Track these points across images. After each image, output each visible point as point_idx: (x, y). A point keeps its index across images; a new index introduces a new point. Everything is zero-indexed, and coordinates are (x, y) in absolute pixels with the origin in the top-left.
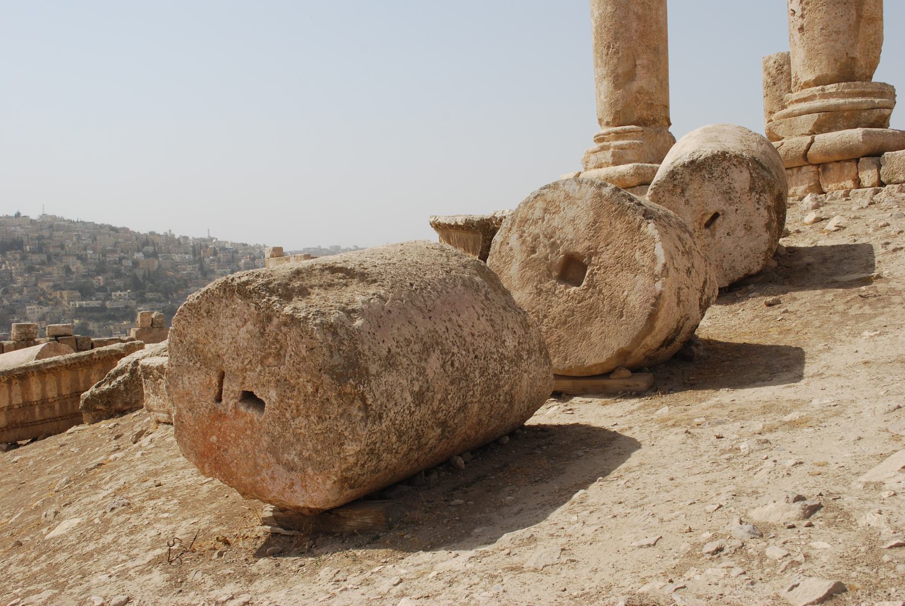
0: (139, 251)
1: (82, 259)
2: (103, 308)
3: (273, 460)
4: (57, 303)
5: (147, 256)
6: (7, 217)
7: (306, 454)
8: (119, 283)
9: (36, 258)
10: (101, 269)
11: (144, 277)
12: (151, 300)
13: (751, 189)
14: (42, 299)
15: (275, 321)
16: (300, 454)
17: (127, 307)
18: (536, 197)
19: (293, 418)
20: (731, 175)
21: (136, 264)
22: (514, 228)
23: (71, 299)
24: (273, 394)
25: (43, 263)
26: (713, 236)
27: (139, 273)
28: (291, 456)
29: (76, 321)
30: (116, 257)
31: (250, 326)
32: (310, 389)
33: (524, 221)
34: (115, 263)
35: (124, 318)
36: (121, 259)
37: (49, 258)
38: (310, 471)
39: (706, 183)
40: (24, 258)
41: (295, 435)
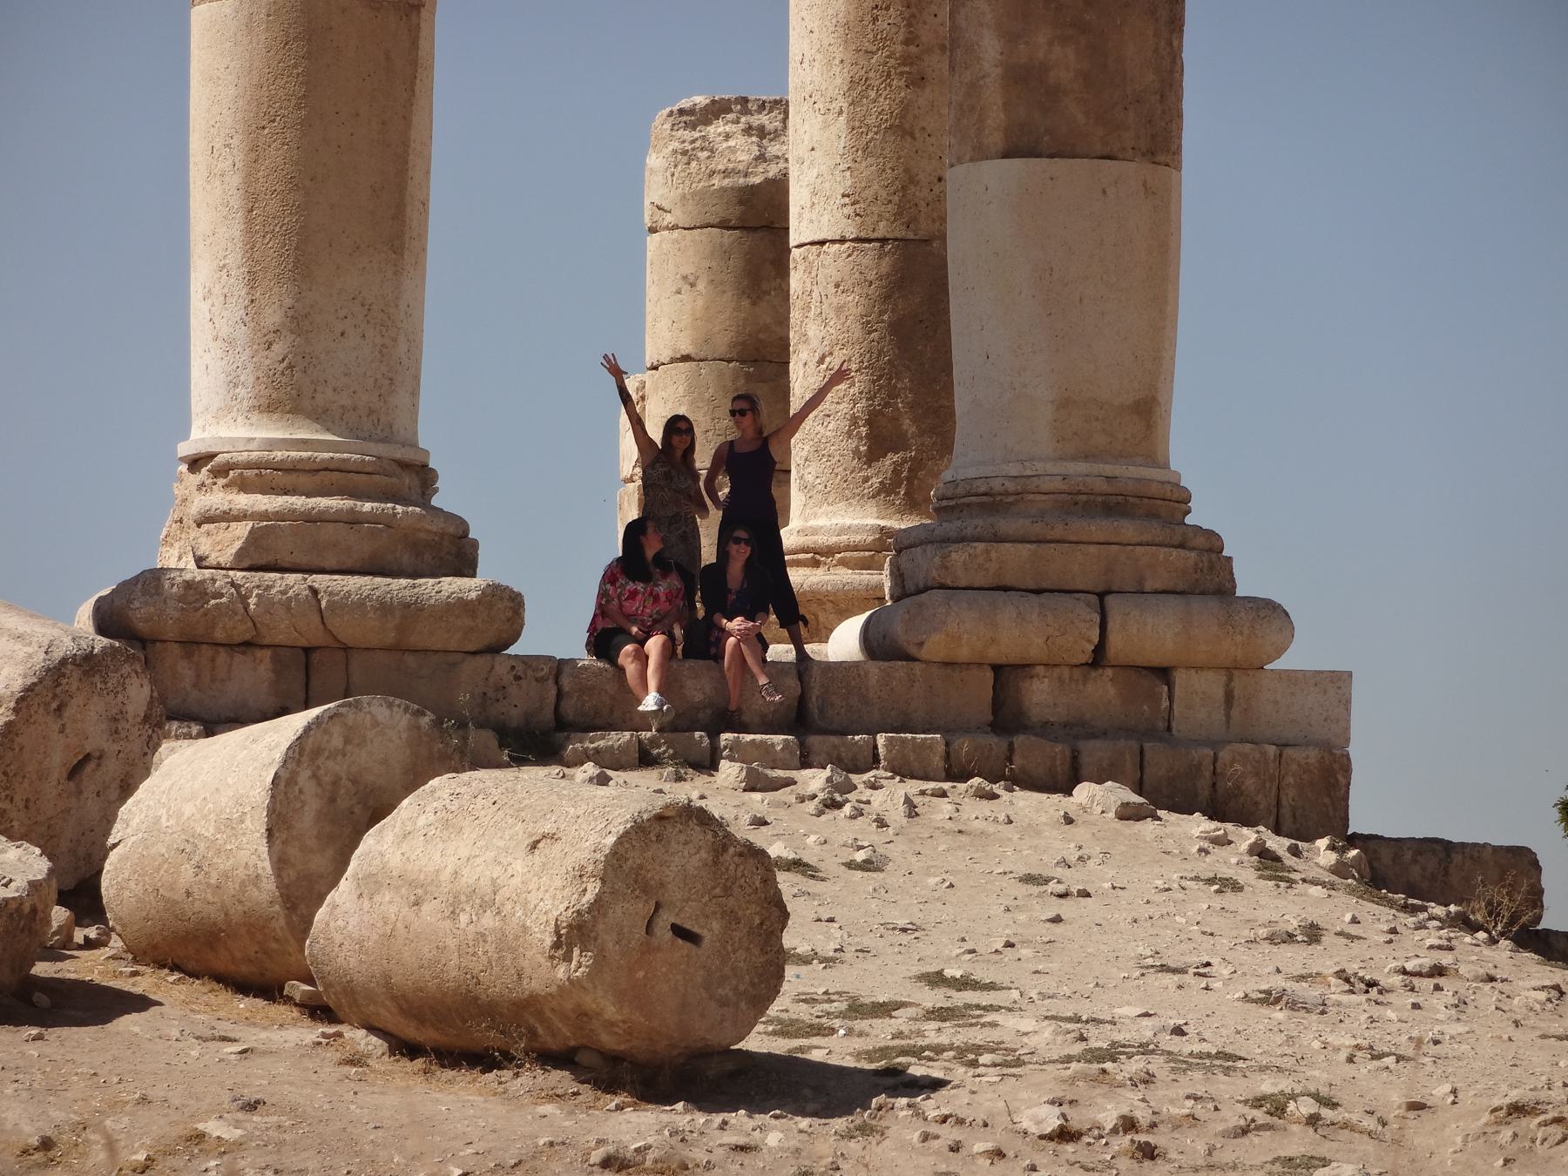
3: (705, 995)
7: (742, 988)
13: (146, 718)
15: (732, 850)
16: (736, 988)
18: (331, 718)
19: (735, 951)
20: (129, 689)
22: (304, 759)
24: (716, 925)
26: (80, 792)
28: (725, 991)
31: (703, 854)
32: (757, 921)
33: (317, 752)
38: (743, 1005)
39: (95, 698)
41: (733, 969)
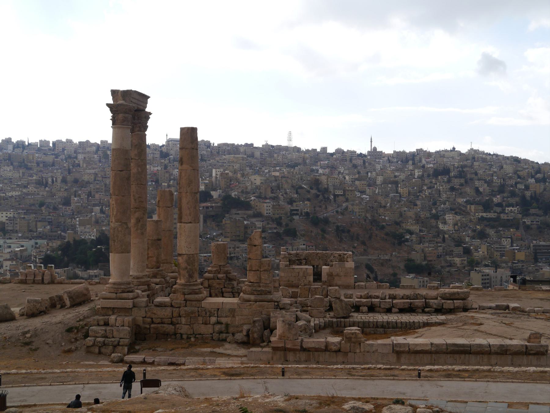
0: (532, 177)
1: (489, 183)
2: (498, 219)
4: (468, 213)
5: (538, 181)
6: (446, 151)
8: (512, 200)
9: (456, 182)
10: (501, 189)
11: (531, 196)
12: (533, 215)
14: (456, 210)
17: (514, 218)
21: (527, 188)
23: (476, 211)
25: (461, 185)
27: (528, 194)
29: (478, 227)
30: (513, 182)
34: (512, 186)
35: (511, 226)
36: (516, 183)
37: (466, 182)
40: (449, 181)
